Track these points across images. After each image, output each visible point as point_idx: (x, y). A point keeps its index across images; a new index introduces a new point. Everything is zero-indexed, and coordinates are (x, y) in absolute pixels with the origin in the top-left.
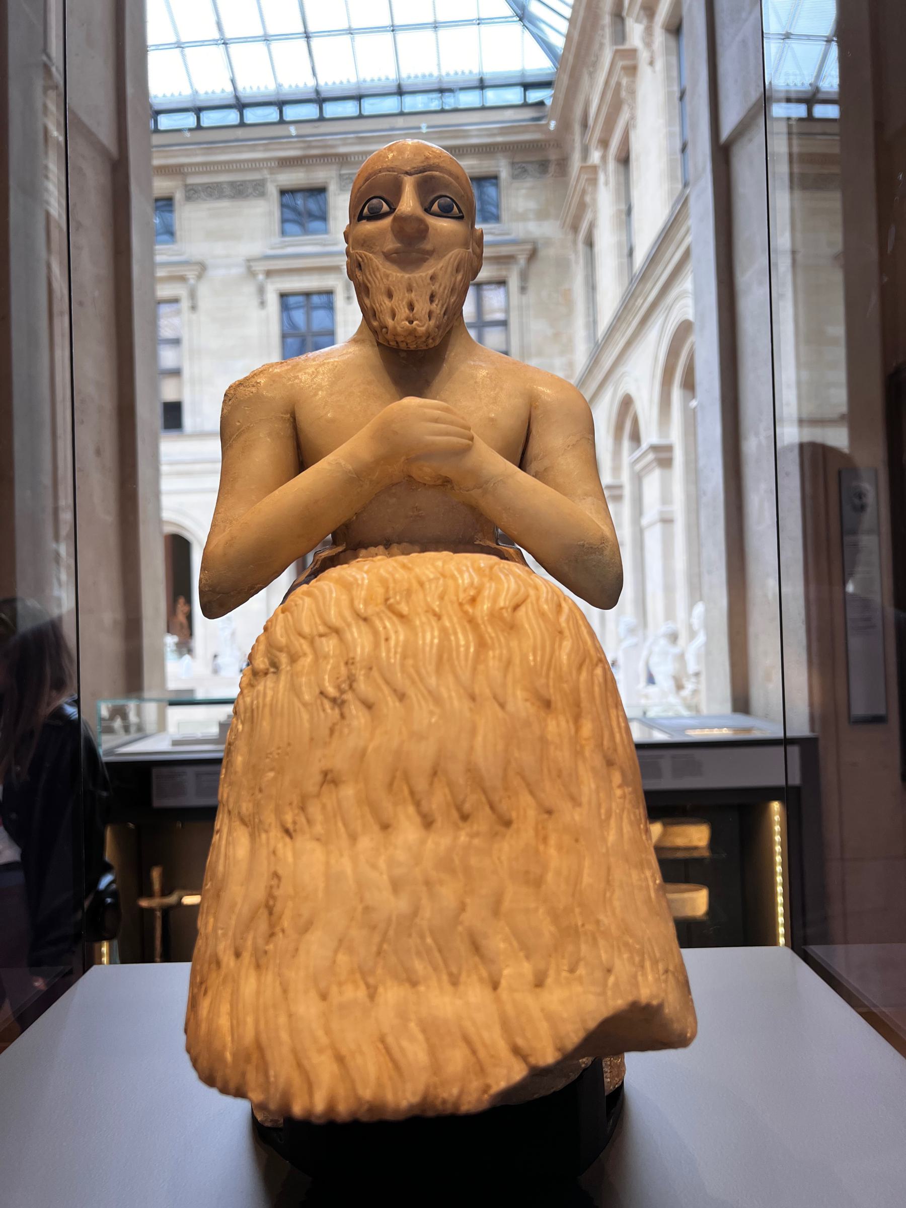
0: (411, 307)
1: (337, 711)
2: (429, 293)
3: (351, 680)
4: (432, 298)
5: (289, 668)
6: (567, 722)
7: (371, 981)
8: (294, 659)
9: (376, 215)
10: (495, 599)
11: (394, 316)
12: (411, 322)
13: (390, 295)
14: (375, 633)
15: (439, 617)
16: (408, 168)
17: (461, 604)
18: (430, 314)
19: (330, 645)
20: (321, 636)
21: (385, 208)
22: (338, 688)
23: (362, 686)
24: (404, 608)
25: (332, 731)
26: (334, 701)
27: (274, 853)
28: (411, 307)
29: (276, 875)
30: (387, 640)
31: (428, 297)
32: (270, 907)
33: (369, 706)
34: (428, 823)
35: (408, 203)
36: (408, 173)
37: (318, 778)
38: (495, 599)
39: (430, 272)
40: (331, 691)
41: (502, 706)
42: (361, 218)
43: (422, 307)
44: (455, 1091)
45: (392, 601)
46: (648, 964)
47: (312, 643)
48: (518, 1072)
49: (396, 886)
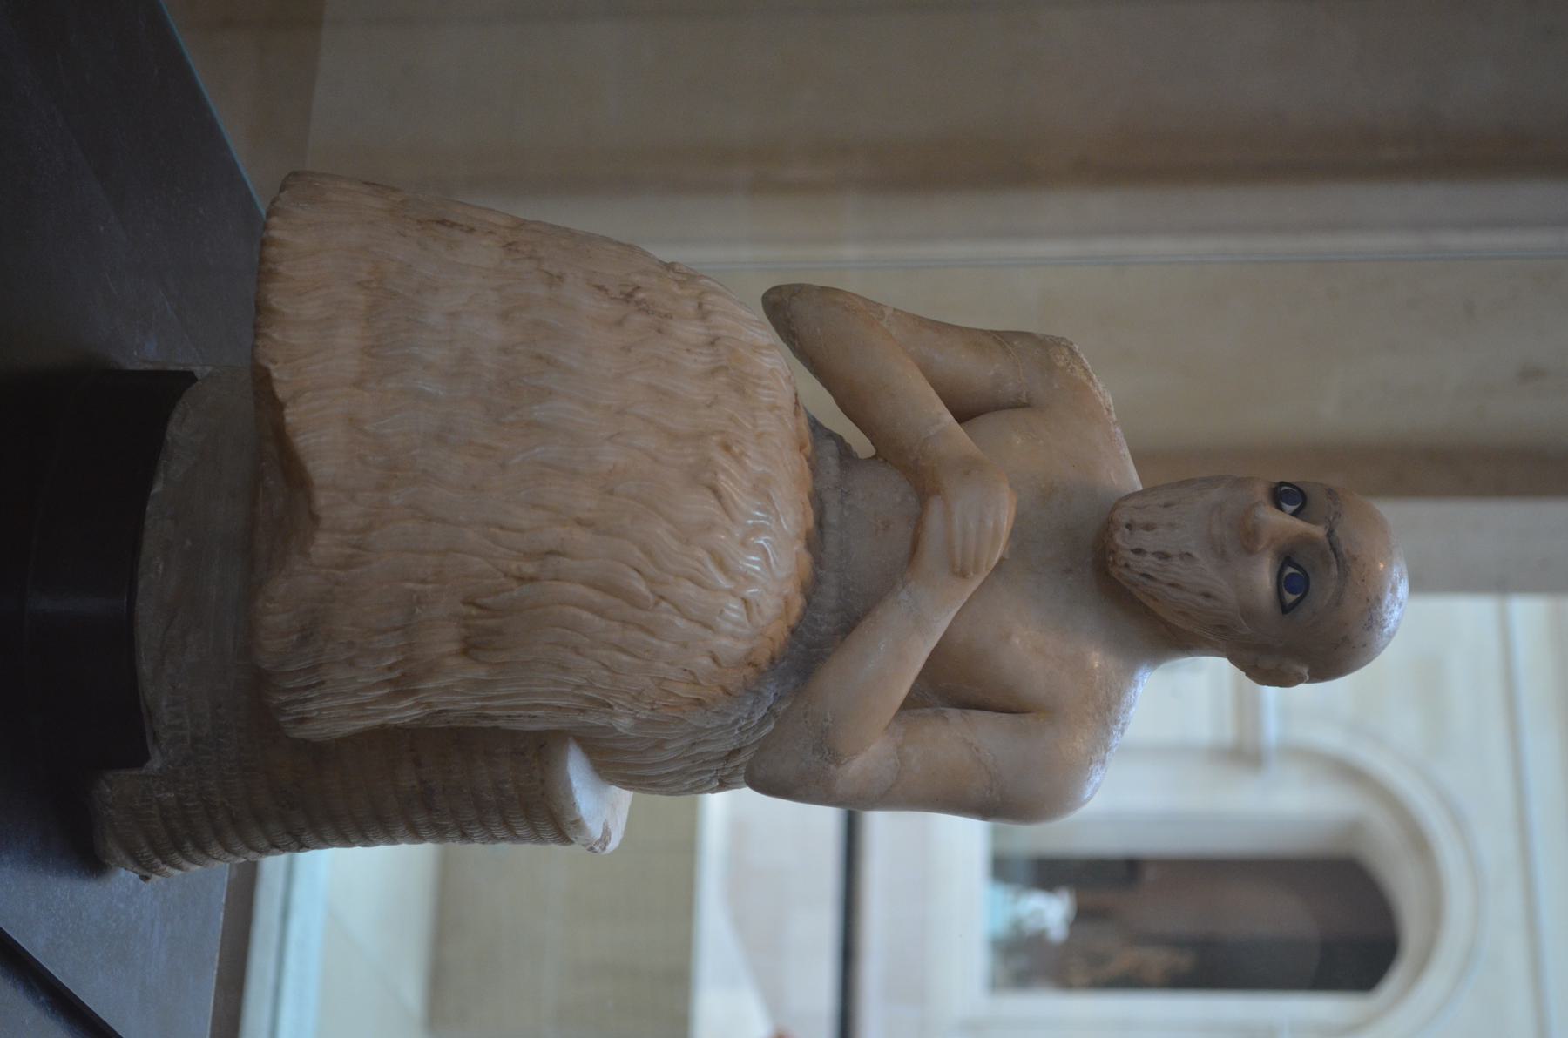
0: (1149, 527)
2: (1169, 551)
3: (647, 312)
4: (1164, 556)
6: (590, 510)
7: (374, 285)
10: (724, 470)
12: (1129, 526)
13: (1166, 506)
15: (709, 406)
16: (1337, 532)
18: (1138, 551)
22: (643, 300)
23: (639, 319)
25: (600, 288)
31: (1161, 549)
33: (620, 323)
34: (504, 350)
35: (1280, 522)
36: (1330, 534)
37: (555, 271)
38: (730, 476)
39: (1196, 554)
40: (640, 295)
43: (1146, 540)
44: (276, 336)
46: (349, 551)
48: (282, 392)
49: (453, 315)
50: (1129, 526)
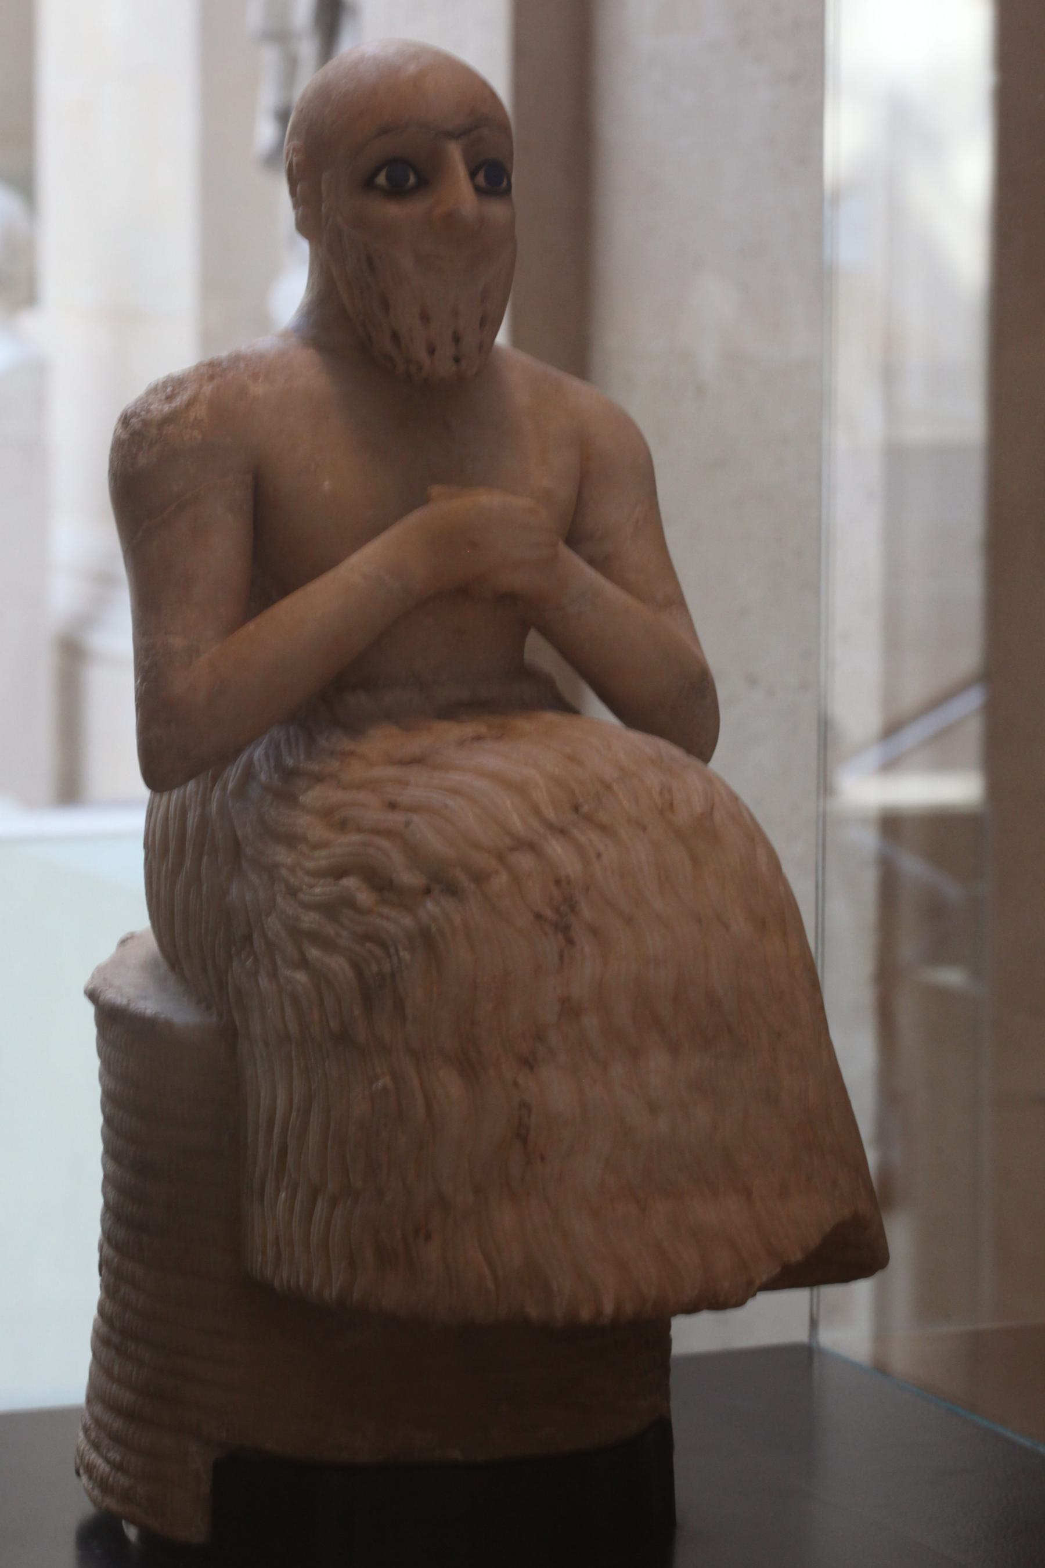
0: (457, 339)
1: (560, 936)
5: (473, 886)
8: (480, 878)
9: (397, 191)
11: (432, 351)
14: (580, 850)
17: (661, 812)
19: (525, 861)
20: (512, 849)
21: (412, 180)
22: (557, 910)
24: (603, 817)
26: (556, 926)
27: (516, 1084)
28: (457, 339)
29: (525, 1105)
30: (599, 855)
32: (522, 1134)
41: (727, 927)
42: (368, 184)
45: (586, 808)
47: (501, 858)
49: (653, 1108)
50: (457, 360)
